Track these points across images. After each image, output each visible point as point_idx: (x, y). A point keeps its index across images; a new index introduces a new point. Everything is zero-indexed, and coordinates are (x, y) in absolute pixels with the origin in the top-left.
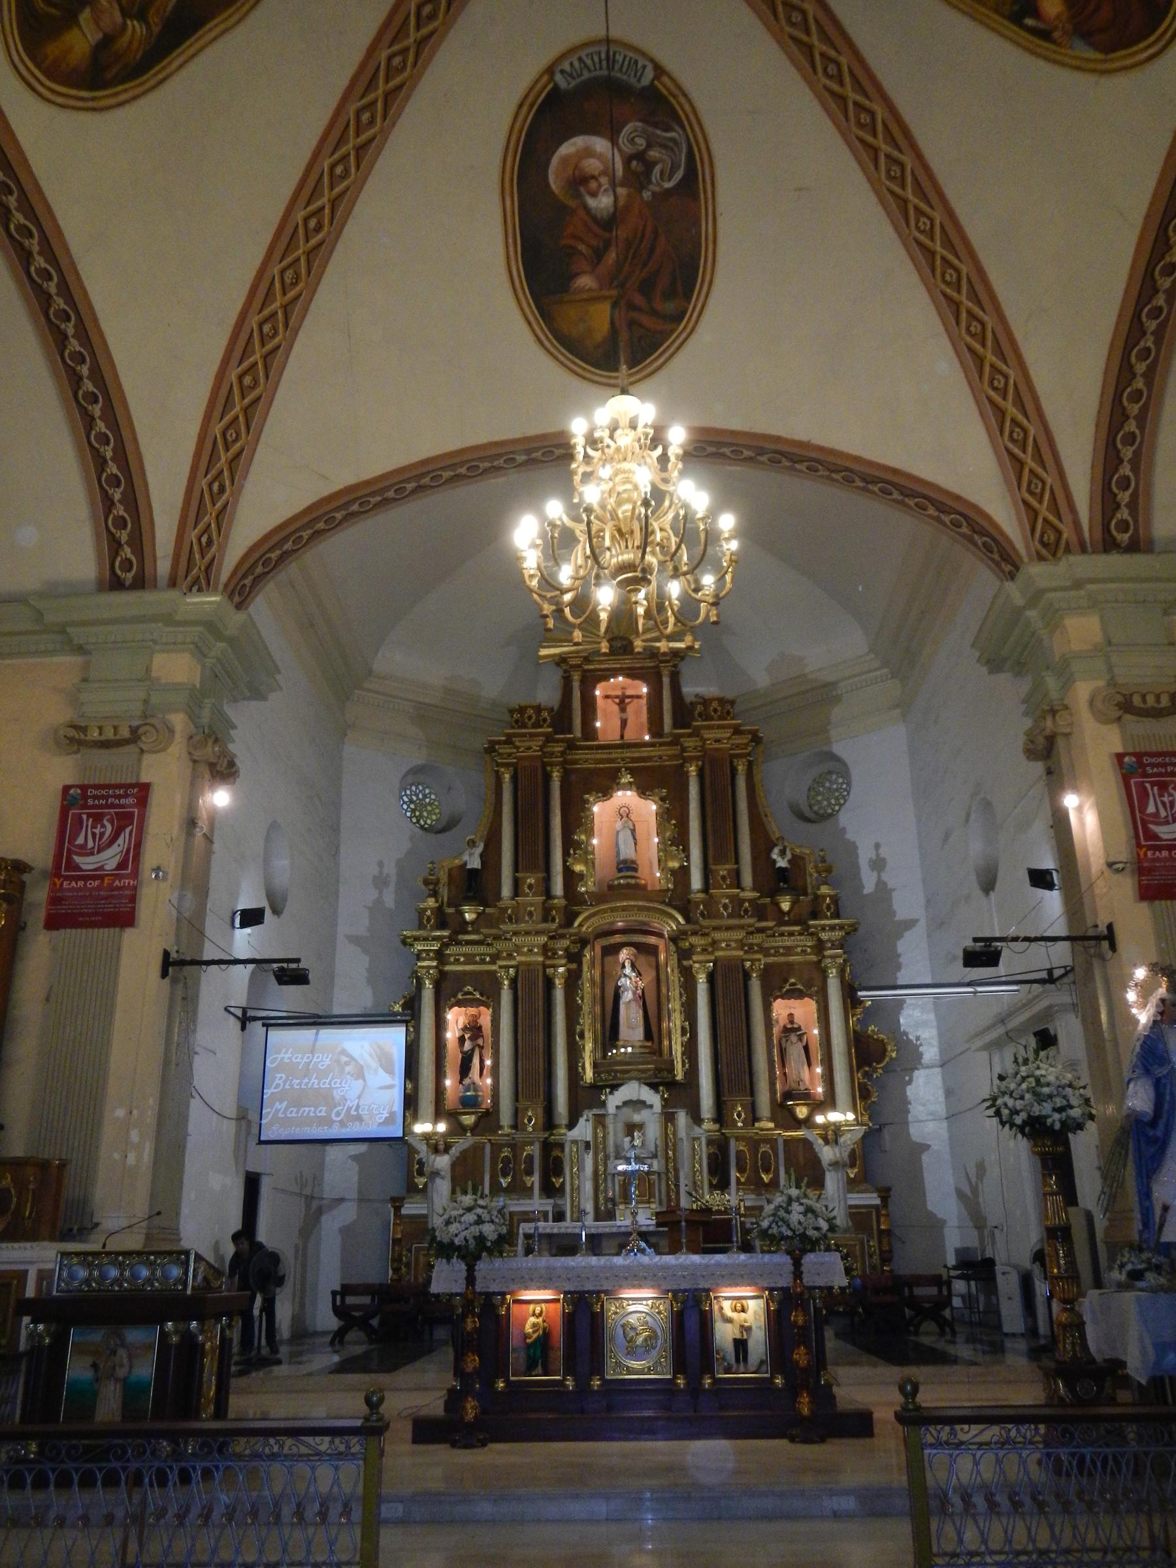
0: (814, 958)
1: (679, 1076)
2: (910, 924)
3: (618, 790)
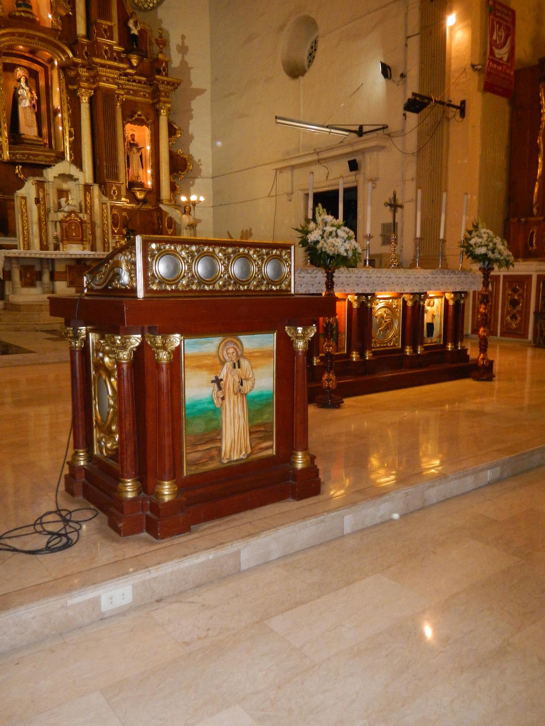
0: (150, 101)
2: (201, 92)
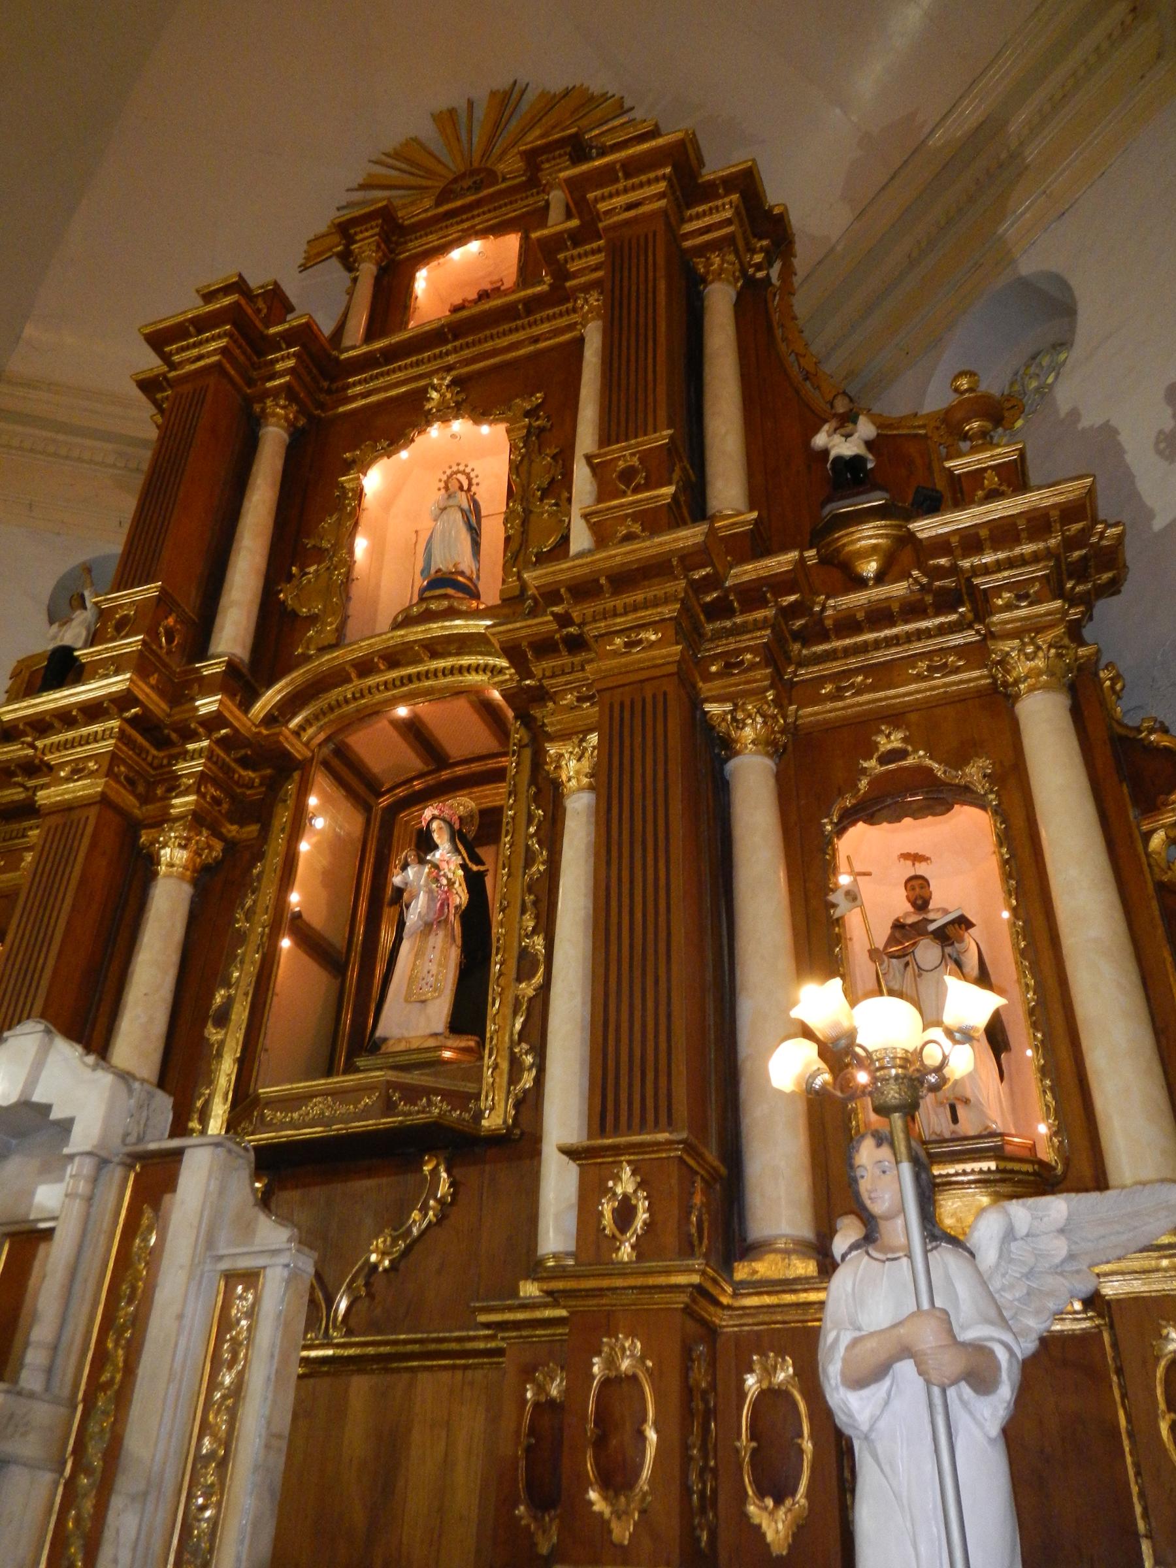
3: (429, 423)
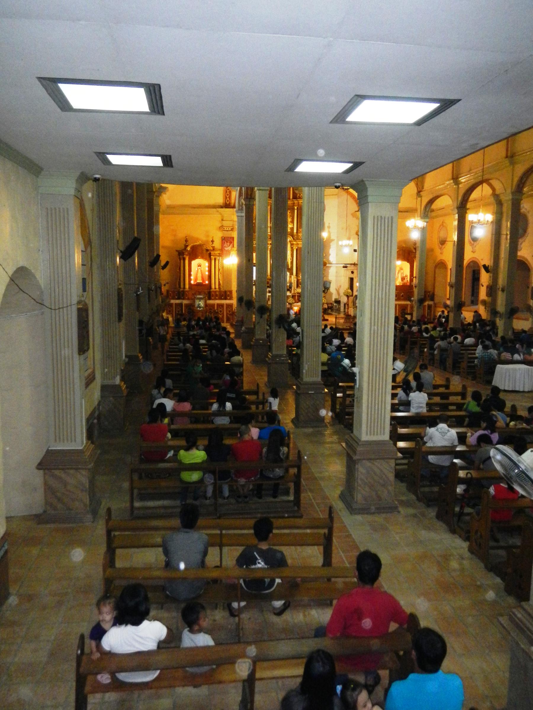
1: (290, 267)
2: (333, 240)
